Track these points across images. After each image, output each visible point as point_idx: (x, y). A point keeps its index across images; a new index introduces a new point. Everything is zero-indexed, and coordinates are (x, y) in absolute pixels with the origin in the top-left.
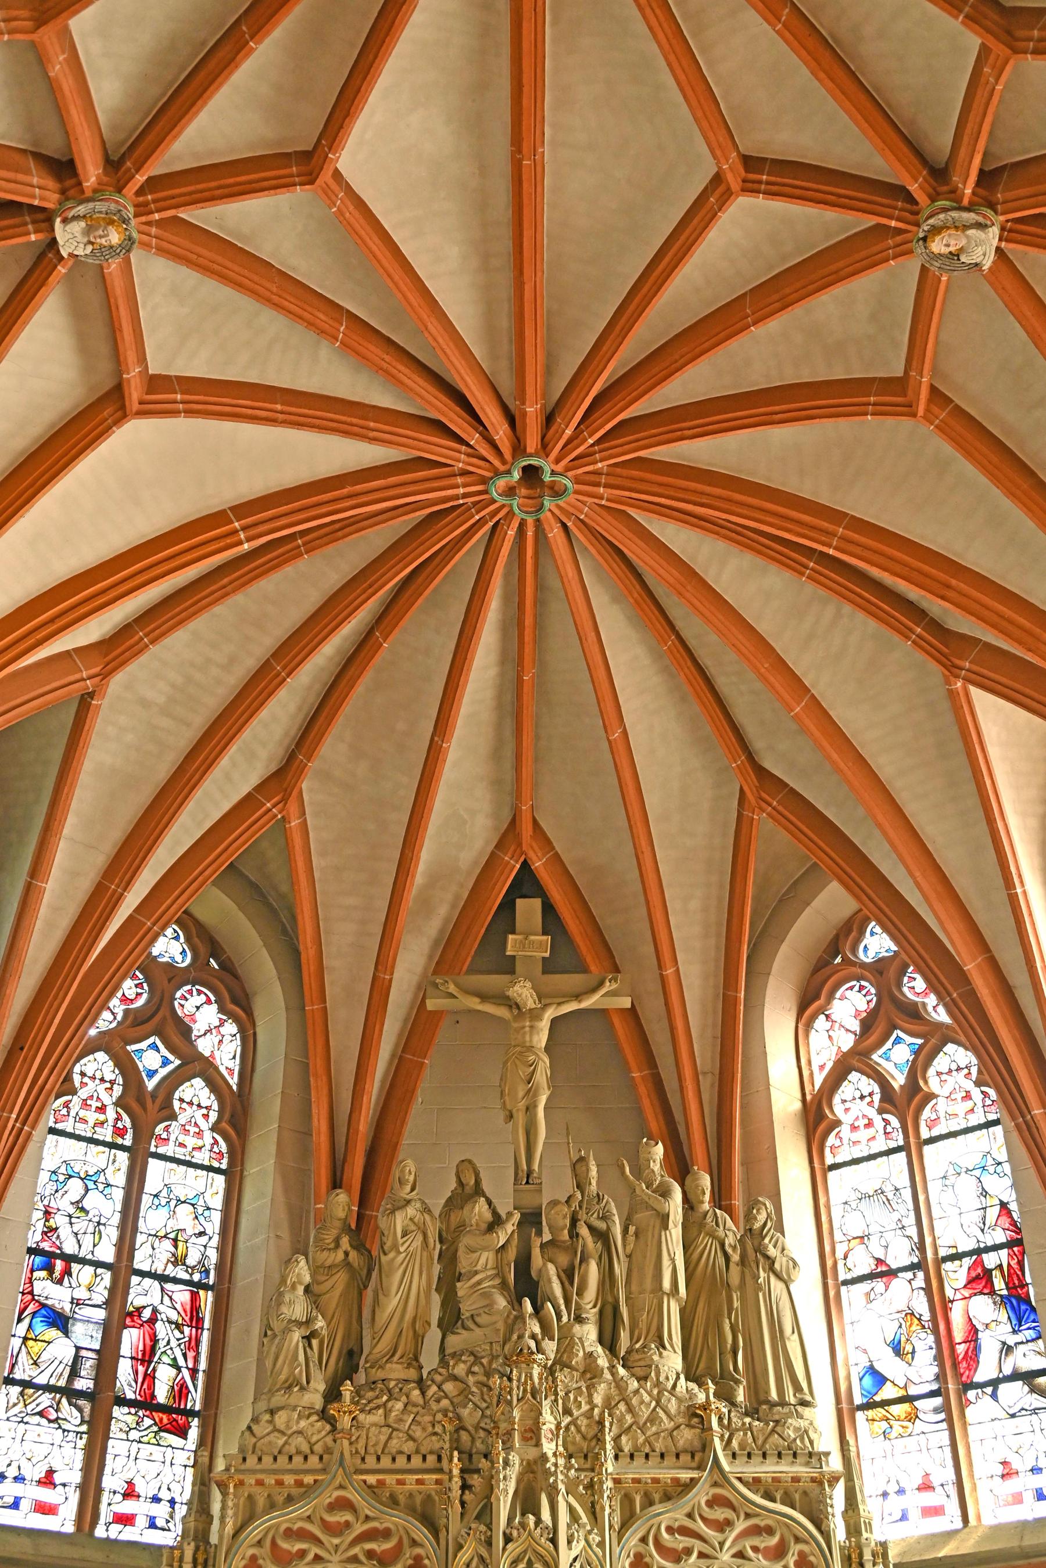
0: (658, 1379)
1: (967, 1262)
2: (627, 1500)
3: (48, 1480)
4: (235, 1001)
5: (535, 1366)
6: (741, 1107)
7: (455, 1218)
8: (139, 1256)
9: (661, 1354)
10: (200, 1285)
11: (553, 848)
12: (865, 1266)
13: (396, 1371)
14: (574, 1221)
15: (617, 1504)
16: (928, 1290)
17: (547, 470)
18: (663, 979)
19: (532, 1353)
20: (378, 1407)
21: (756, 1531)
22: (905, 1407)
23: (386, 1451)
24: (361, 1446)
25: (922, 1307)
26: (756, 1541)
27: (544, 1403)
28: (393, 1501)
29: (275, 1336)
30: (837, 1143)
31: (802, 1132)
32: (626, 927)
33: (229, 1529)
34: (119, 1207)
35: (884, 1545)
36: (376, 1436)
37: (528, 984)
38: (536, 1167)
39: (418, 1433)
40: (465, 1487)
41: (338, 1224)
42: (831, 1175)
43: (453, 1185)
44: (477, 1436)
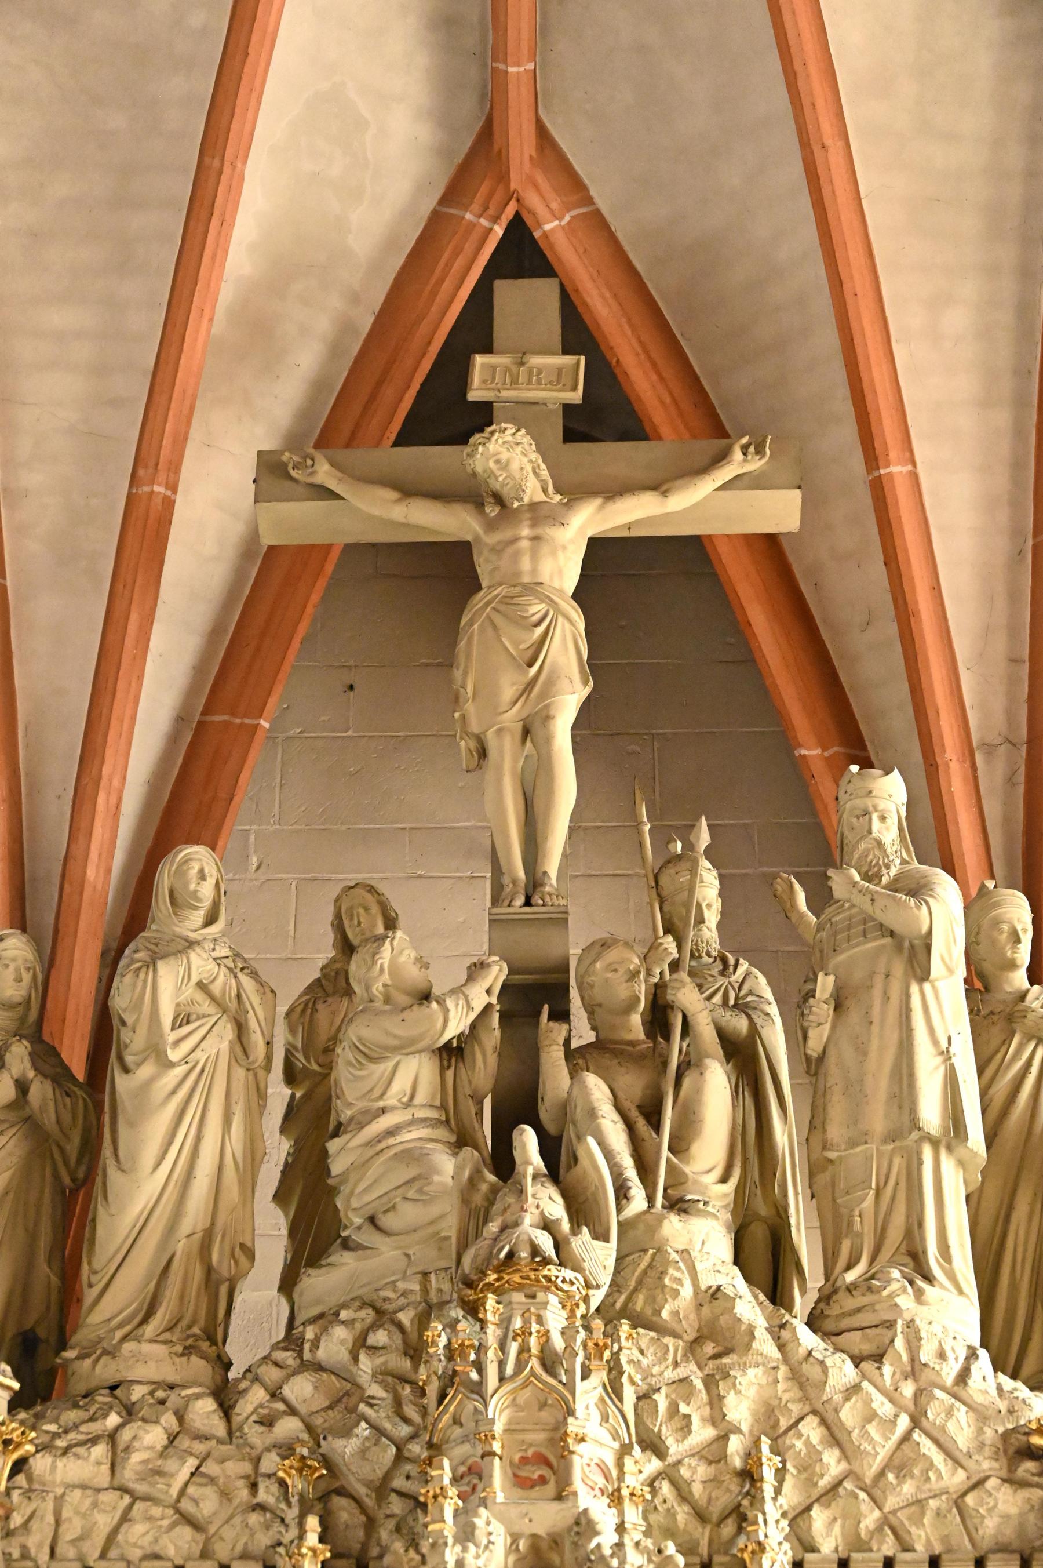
0: (913, 1359)
5: (553, 1299)
9: (919, 1294)
13: (148, 1361)
19: (546, 1262)
20: (94, 1441)
23: (113, 1553)
27: (580, 1386)
36: (84, 1516)
38: (552, 864)
39: (206, 1503)
44: (380, 1515)
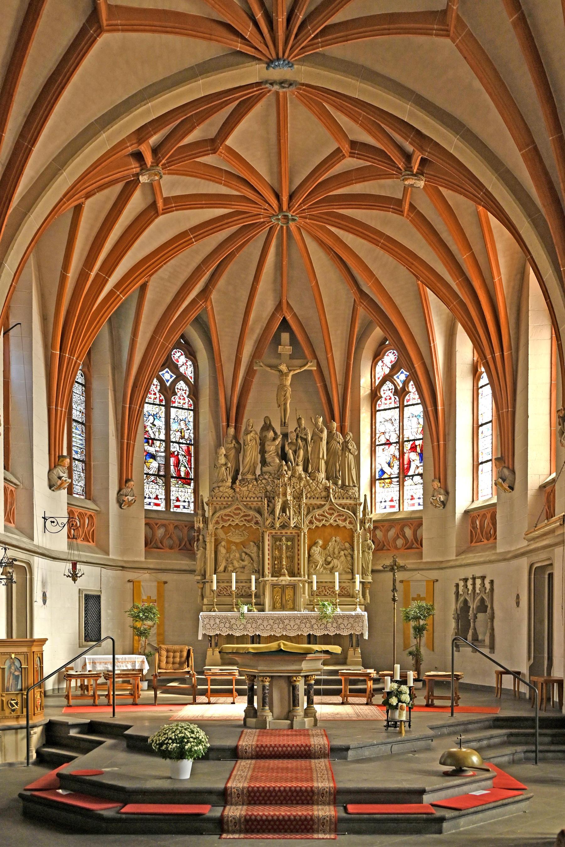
1: (411, 443)
2: (309, 508)
3: (157, 498)
4: (191, 354)
7: (265, 433)
8: (172, 437)
10: (189, 444)
11: (293, 311)
12: (383, 441)
13: (249, 477)
14: (297, 436)
15: (306, 509)
16: (399, 449)
18: (327, 358)
21: (340, 515)
22: (389, 480)
25: (397, 454)
26: (339, 518)
28: (251, 508)
30: (380, 403)
31: (370, 400)
33: (211, 514)
38: (287, 421)
39: (256, 492)
40: (268, 506)
42: (378, 413)
43: (263, 423)
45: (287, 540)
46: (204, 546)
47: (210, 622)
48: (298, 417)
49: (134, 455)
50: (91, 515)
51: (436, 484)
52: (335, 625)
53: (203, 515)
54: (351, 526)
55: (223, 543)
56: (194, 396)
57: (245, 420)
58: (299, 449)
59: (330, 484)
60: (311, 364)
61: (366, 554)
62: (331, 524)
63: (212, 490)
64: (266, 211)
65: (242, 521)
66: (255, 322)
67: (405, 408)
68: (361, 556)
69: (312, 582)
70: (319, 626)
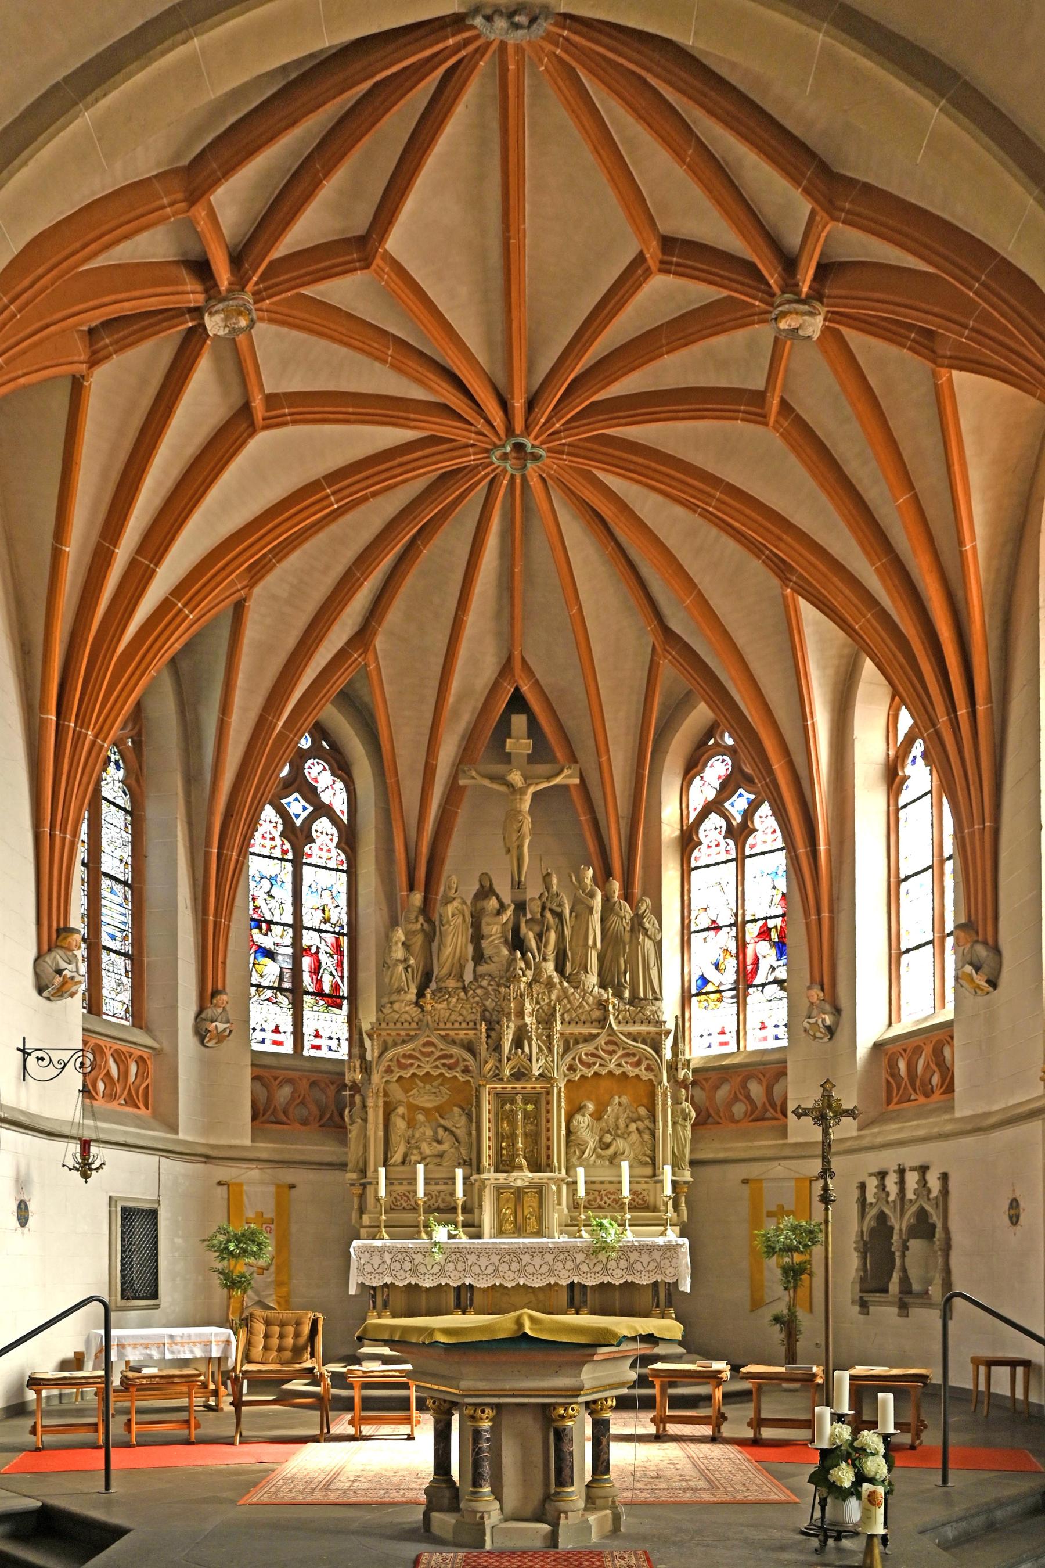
2: (566, 1043)
6: (644, 834)
7: (479, 905)
12: (706, 924)
13: (451, 983)
14: (544, 908)
15: (561, 1044)
16: (736, 938)
17: (529, 445)
21: (627, 1055)
24: (436, 1018)
25: (732, 946)
26: (627, 1059)
28: (453, 1042)
29: (389, 967)
31: (679, 849)
32: (578, 725)
33: (376, 1054)
34: (291, 894)
35: (689, 1061)
37: (519, 773)
38: (523, 879)
39: (464, 1012)
40: (488, 1037)
41: (417, 909)
42: (693, 873)
43: (477, 886)
45: (526, 1101)
46: (363, 1116)
47: (374, 1258)
48: (545, 873)
49: (230, 947)
50: (141, 1057)
51: (816, 994)
52: (623, 1264)
53: (363, 1057)
54: (651, 1076)
55: (401, 1110)
56: (347, 843)
57: (443, 880)
58: (548, 929)
59: (608, 995)
60: (570, 772)
61: (679, 1128)
62: (610, 1072)
63: (380, 1008)
64: (481, 437)
65: (437, 1067)
66: (461, 698)
67: (747, 860)
68: (670, 1131)
69: (575, 1183)
70: (591, 1266)
